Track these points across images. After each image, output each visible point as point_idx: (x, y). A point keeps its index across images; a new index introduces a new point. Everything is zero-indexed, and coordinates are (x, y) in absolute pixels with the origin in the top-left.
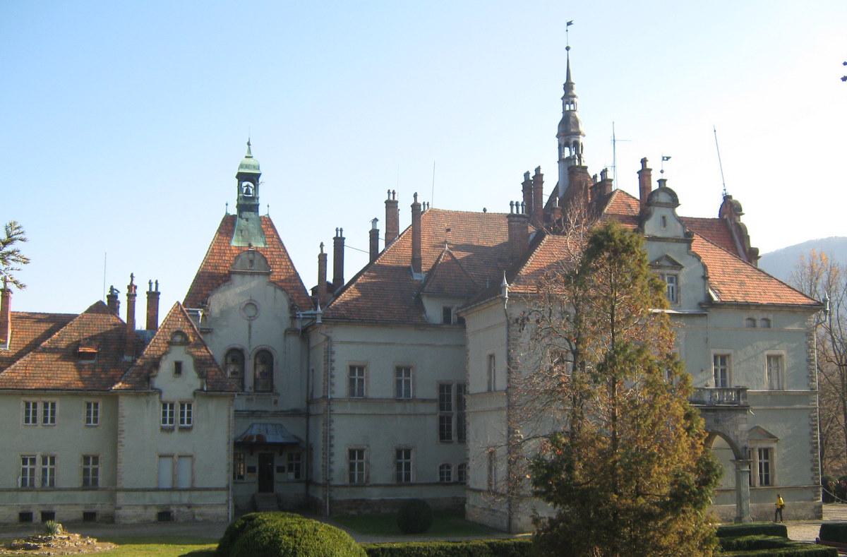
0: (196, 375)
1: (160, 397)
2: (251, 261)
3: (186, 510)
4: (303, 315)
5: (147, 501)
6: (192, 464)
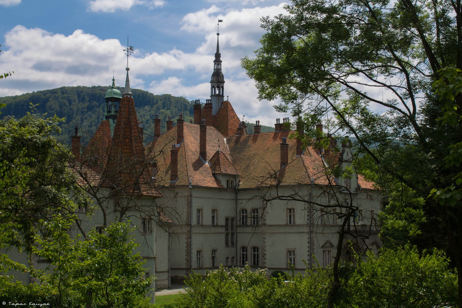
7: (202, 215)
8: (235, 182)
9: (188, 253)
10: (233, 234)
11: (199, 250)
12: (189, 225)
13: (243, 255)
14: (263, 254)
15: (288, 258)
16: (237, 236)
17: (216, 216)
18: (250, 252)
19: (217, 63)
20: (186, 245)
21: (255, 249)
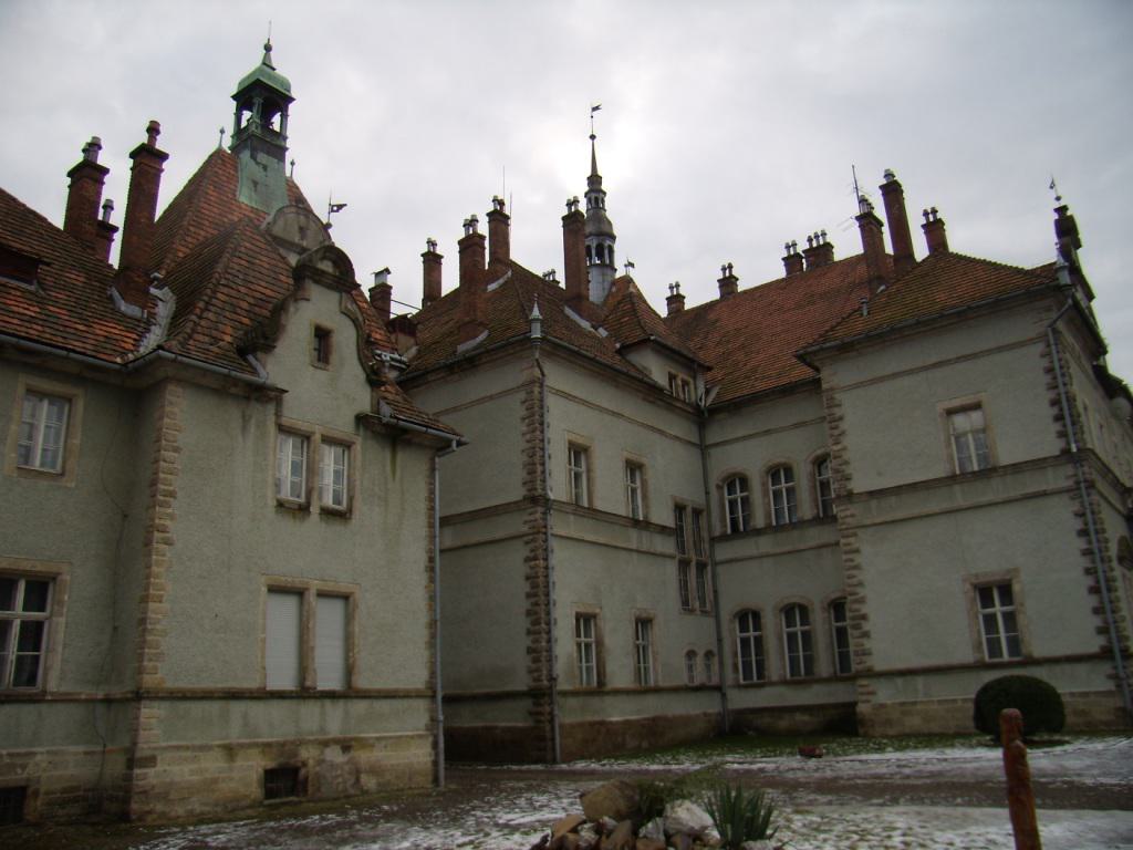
0: (362, 376)
1: (278, 414)
2: (302, 230)
3: (334, 755)
4: (392, 359)
5: (235, 735)
6: (349, 619)
7: (589, 471)
8: (692, 387)
9: (536, 622)
10: (701, 567)
11: (582, 610)
12: (536, 499)
13: (745, 642)
14: (853, 618)
15: (977, 618)
16: (714, 576)
17: (639, 491)
18: (772, 625)
19: (593, 195)
20: (528, 589)
21: (794, 612)
